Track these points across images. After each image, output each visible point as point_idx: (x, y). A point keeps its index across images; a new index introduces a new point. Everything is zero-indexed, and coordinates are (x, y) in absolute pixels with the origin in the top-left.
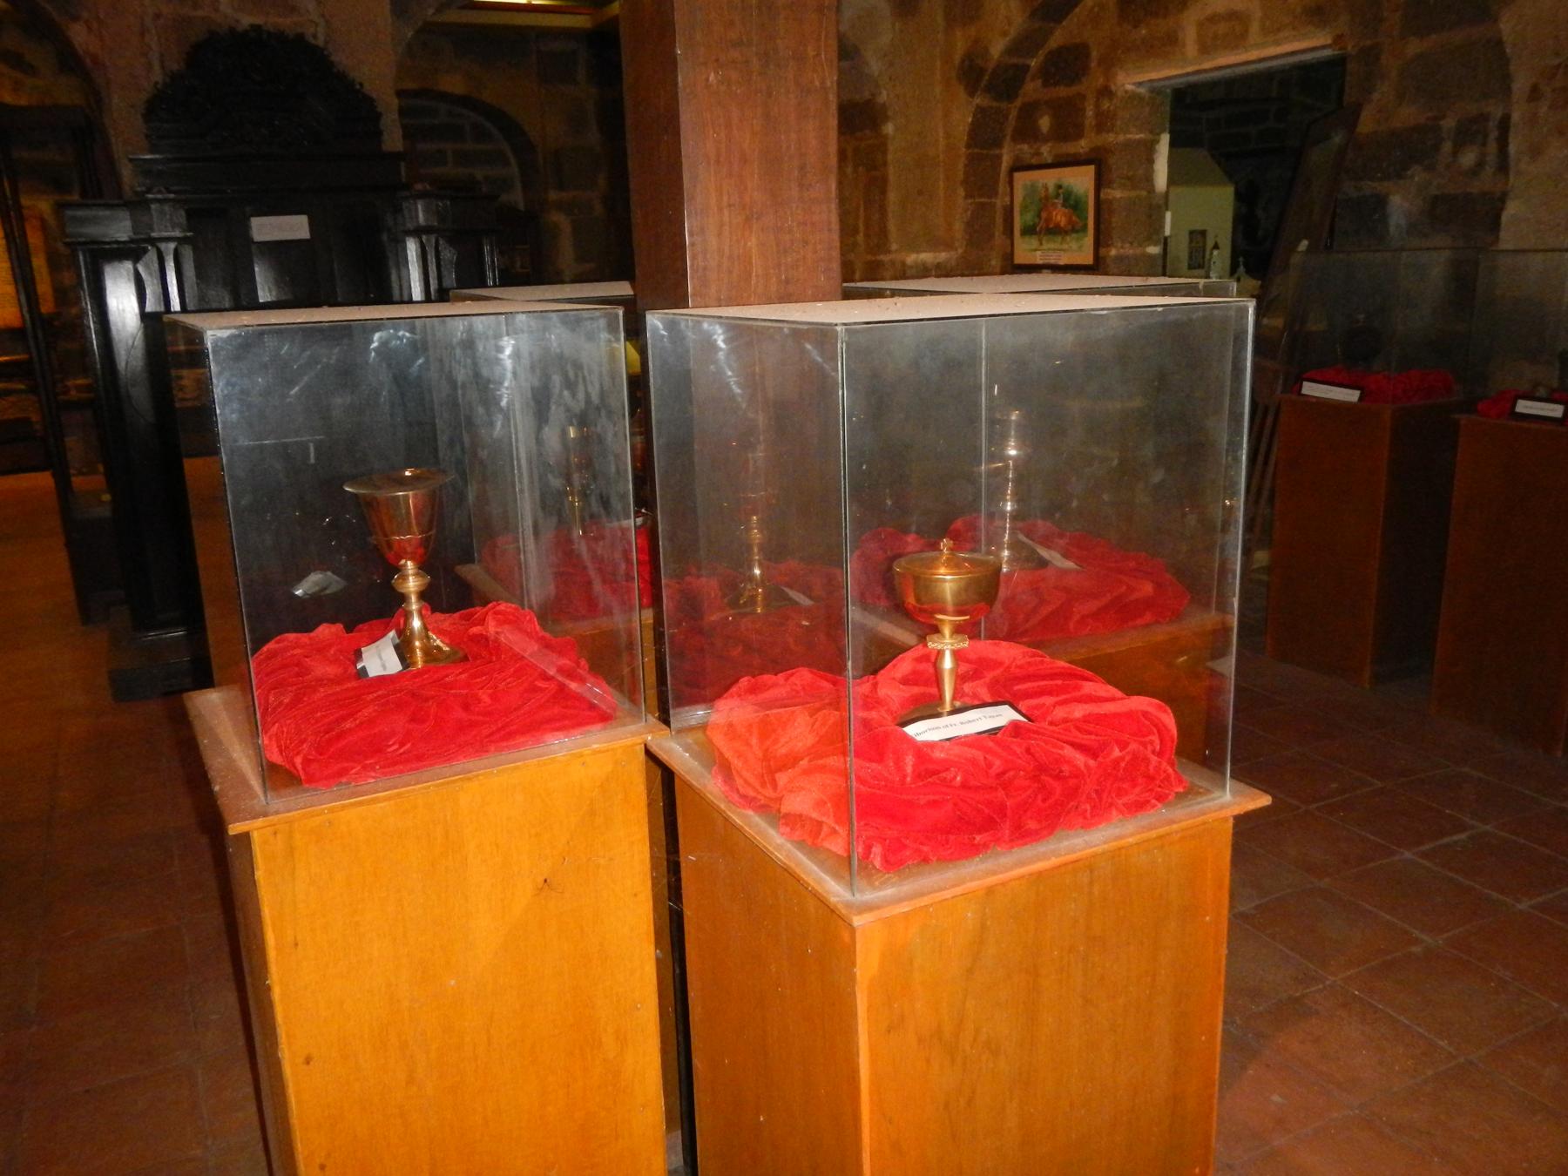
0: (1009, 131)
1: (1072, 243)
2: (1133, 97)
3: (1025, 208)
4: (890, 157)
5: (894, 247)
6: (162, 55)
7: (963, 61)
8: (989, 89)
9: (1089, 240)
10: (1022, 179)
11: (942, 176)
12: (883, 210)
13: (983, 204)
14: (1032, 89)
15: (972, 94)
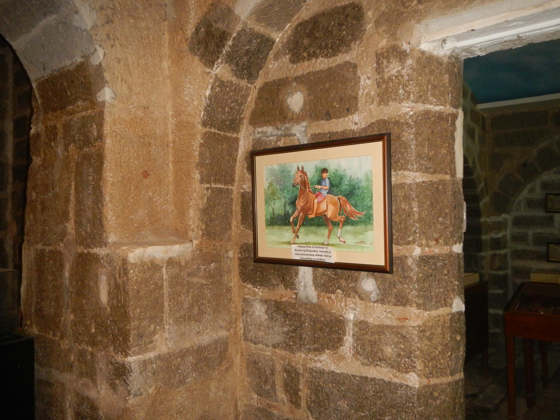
0: (247, 113)
1: (346, 234)
2: (428, 62)
3: (270, 198)
7: (197, 30)
8: (230, 59)
9: (376, 235)
11: (171, 158)
13: (221, 191)
14: (275, 67)
15: (210, 63)
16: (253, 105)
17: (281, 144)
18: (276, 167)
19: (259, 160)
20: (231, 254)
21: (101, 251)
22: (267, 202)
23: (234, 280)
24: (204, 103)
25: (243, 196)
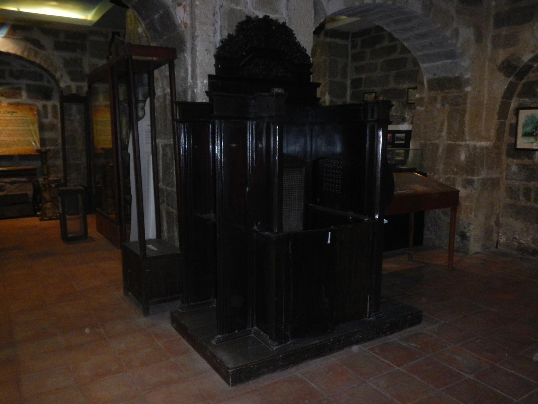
0: (517, 93)
3: (525, 126)
4: (468, 101)
5: (468, 138)
6: (221, 26)
7: (503, 63)
10: (524, 114)
12: (462, 123)
13: (503, 122)
15: (509, 77)
16: (520, 89)
17: (532, 106)
18: (529, 114)
19: (521, 112)
20: (503, 147)
21: (463, 143)
22: (523, 127)
23: (504, 157)
24: (504, 90)
25: (511, 125)
